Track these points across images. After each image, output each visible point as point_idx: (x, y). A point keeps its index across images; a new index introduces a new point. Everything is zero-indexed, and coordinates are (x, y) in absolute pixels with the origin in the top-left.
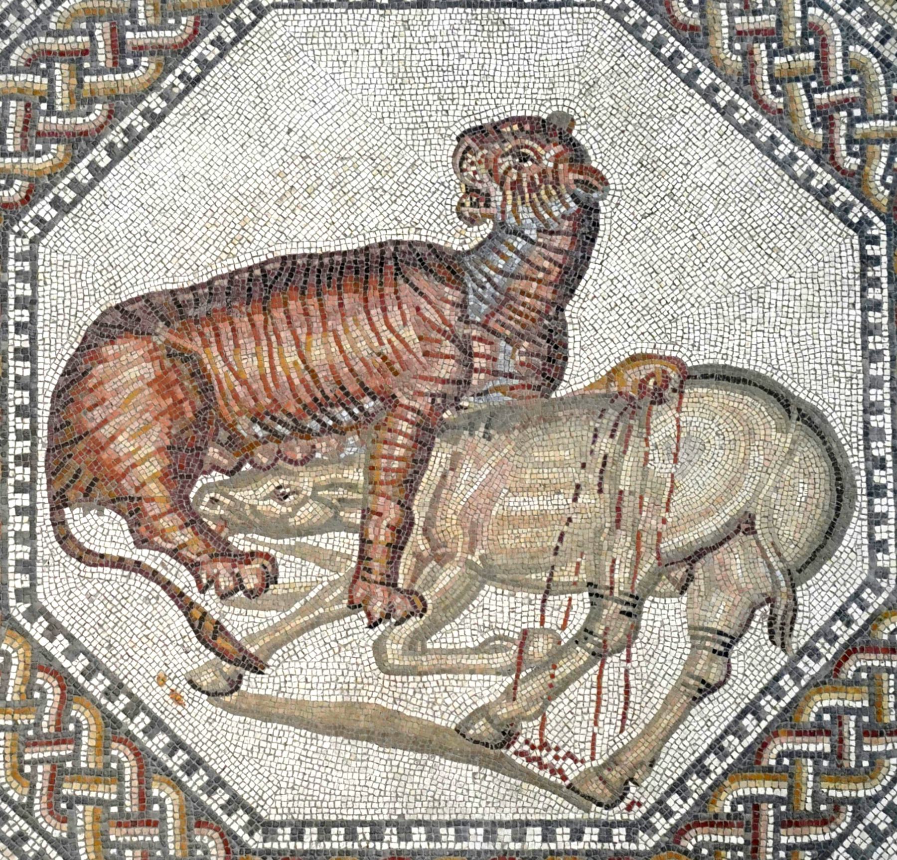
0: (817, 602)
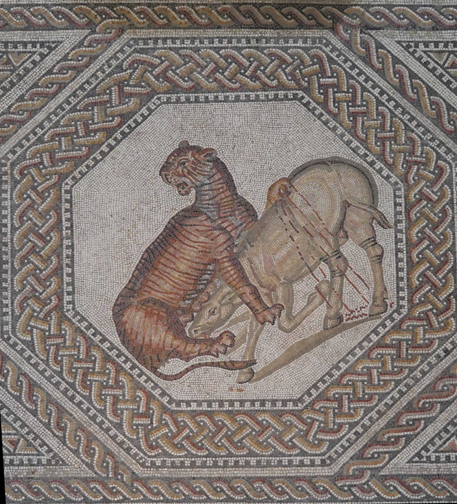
0: (386, 207)
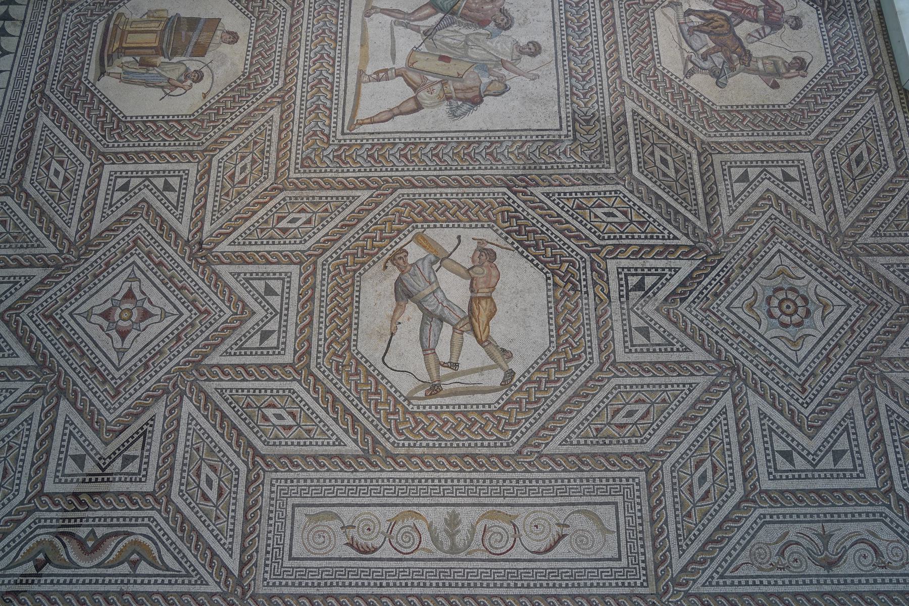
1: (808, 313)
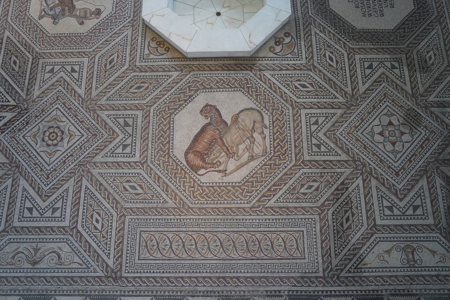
0: (267, 122)
1: (62, 139)
